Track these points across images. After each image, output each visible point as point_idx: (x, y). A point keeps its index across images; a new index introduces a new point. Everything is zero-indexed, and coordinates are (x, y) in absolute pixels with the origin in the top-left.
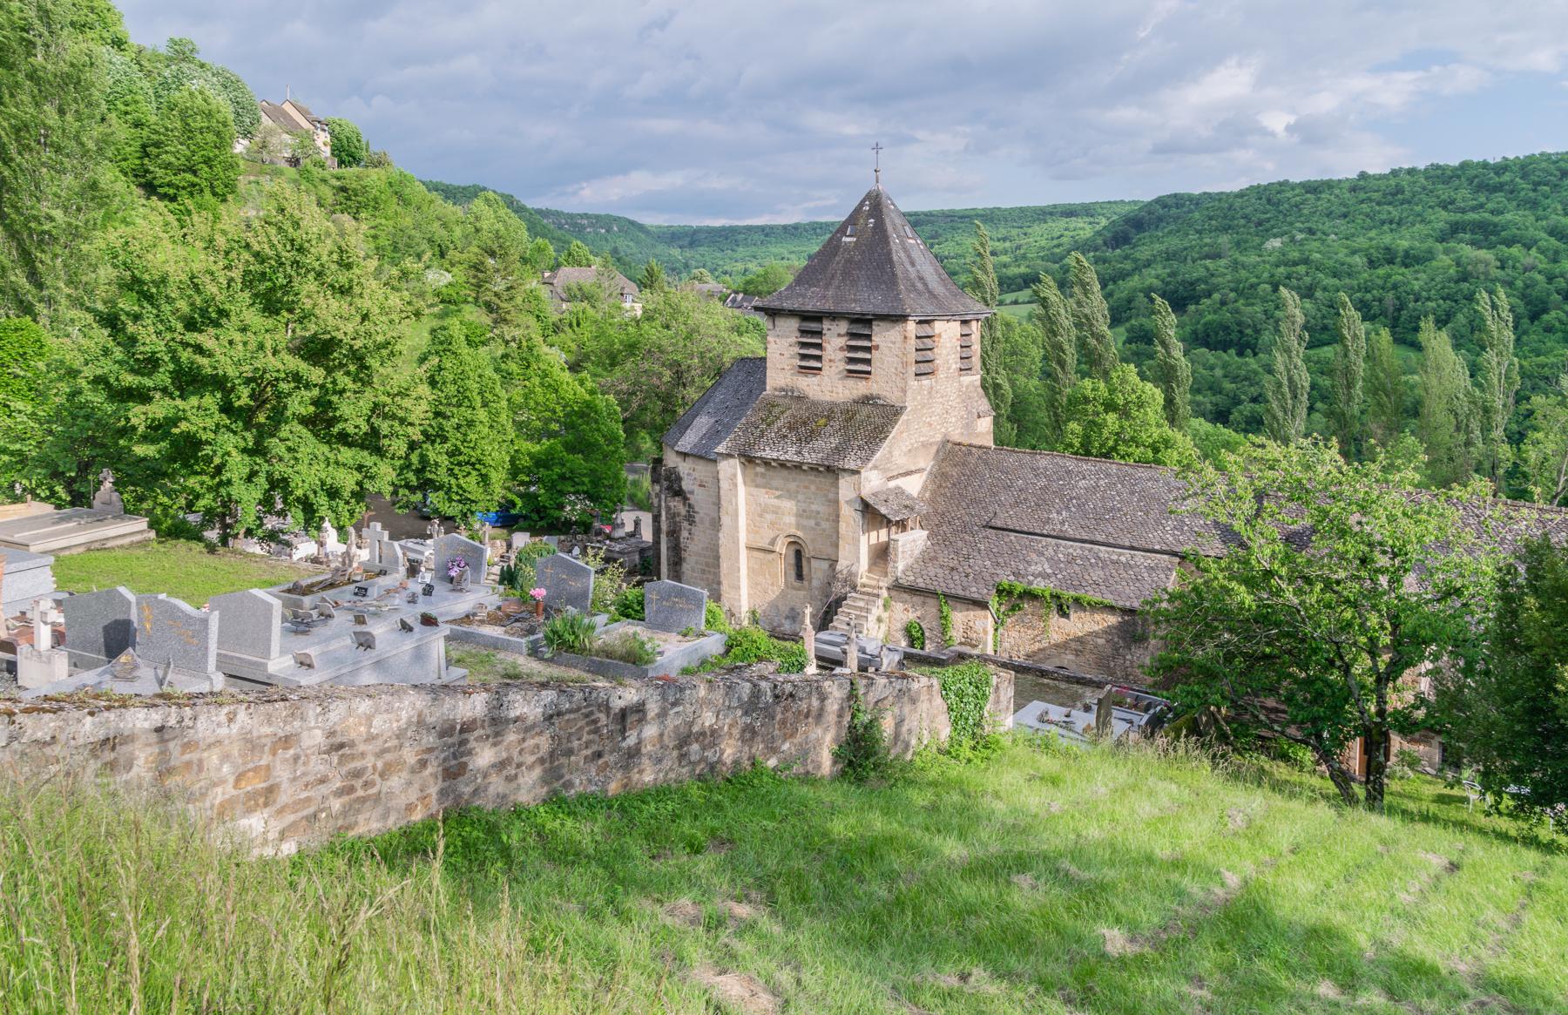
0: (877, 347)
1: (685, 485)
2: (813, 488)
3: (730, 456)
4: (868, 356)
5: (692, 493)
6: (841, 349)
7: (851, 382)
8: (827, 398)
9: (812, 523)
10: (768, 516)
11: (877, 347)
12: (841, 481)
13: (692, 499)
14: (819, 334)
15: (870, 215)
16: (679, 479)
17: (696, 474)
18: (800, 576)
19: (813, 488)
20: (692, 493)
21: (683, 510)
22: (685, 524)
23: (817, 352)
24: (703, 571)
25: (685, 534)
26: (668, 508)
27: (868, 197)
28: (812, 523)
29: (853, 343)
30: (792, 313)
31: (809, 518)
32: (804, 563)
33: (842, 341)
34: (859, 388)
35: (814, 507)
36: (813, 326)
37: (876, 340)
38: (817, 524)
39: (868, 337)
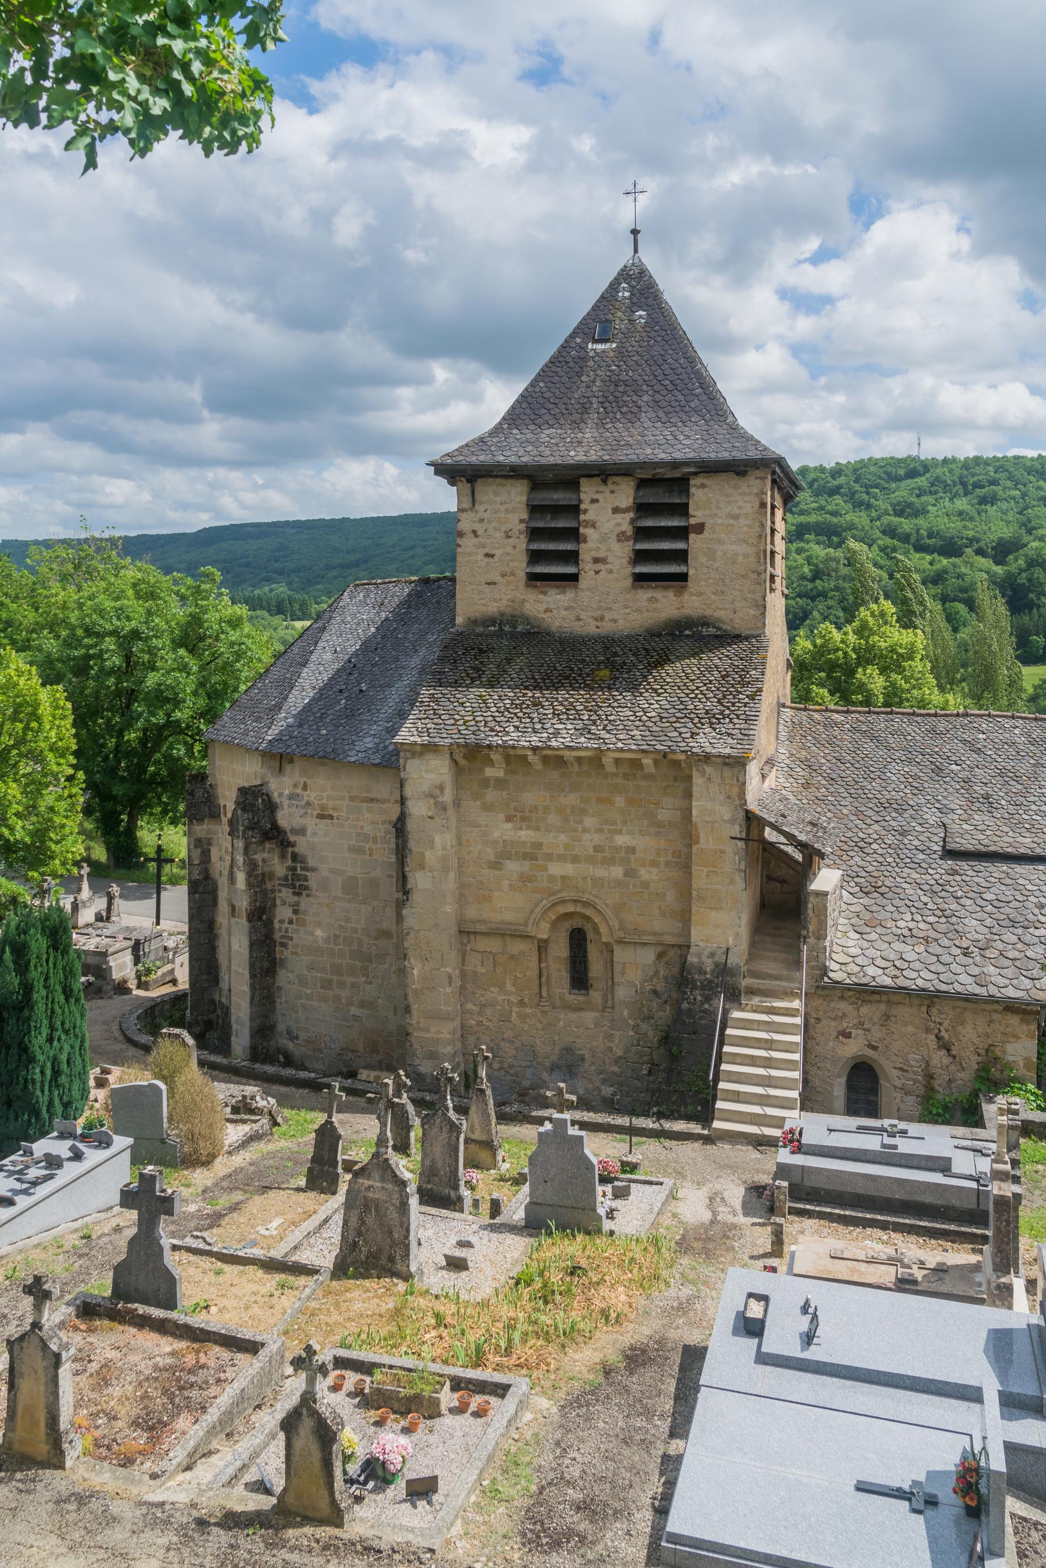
0: (700, 528)
1: (285, 818)
2: (620, 801)
3: (431, 748)
4: (680, 545)
5: (301, 831)
6: (621, 537)
7: (644, 595)
8: (589, 627)
9: (617, 872)
10: (513, 867)
11: (700, 528)
12: (698, 780)
13: (302, 845)
14: (574, 510)
15: (635, 304)
16: (272, 807)
17: (311, 795)
18: (580, 980)
19: (620, 801)
20: (301, 831)
21: (279, 868)
22: (286, 894)
23: (569, 547)
24: (327, 984)
25: (283, 913)
26: (251, 867)
27: (624, 275)
28: (617, 872)
29: (649, 523)
30: (514, 473)
31: (609, 861)
32: (594, 954)
33: (625, 522)
34: (663, 606)
35: (621, 840)
36: (560, 497)
37: (697, 514)
38: (630, 873)
39: (683, 510)
